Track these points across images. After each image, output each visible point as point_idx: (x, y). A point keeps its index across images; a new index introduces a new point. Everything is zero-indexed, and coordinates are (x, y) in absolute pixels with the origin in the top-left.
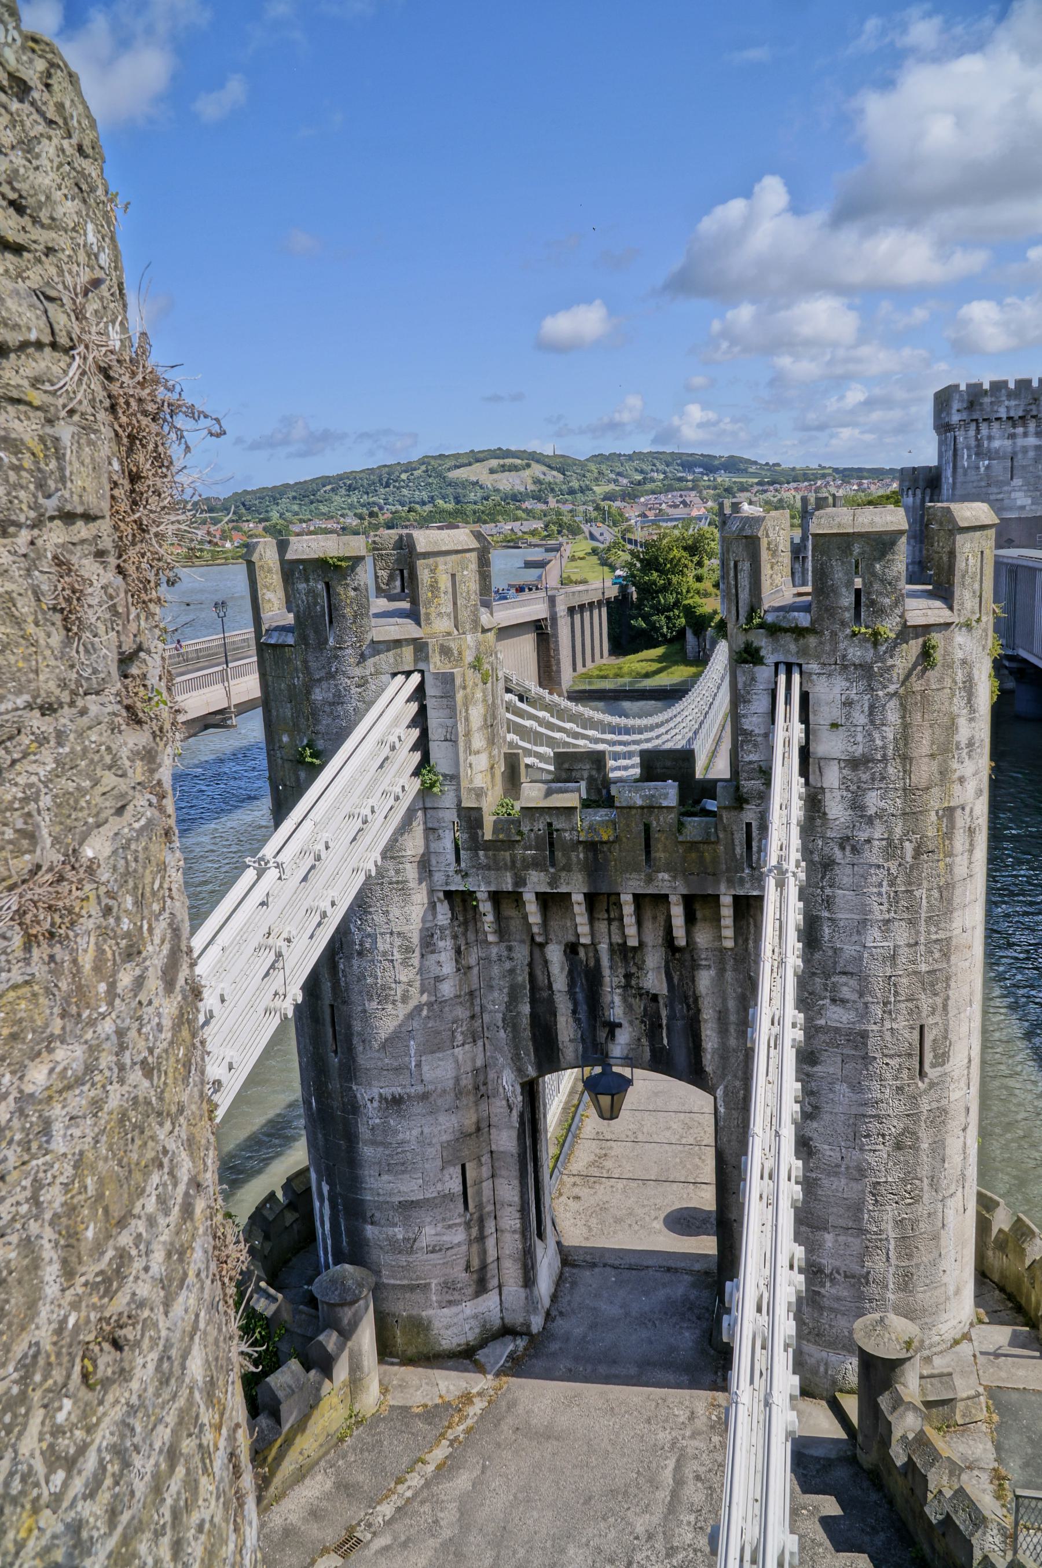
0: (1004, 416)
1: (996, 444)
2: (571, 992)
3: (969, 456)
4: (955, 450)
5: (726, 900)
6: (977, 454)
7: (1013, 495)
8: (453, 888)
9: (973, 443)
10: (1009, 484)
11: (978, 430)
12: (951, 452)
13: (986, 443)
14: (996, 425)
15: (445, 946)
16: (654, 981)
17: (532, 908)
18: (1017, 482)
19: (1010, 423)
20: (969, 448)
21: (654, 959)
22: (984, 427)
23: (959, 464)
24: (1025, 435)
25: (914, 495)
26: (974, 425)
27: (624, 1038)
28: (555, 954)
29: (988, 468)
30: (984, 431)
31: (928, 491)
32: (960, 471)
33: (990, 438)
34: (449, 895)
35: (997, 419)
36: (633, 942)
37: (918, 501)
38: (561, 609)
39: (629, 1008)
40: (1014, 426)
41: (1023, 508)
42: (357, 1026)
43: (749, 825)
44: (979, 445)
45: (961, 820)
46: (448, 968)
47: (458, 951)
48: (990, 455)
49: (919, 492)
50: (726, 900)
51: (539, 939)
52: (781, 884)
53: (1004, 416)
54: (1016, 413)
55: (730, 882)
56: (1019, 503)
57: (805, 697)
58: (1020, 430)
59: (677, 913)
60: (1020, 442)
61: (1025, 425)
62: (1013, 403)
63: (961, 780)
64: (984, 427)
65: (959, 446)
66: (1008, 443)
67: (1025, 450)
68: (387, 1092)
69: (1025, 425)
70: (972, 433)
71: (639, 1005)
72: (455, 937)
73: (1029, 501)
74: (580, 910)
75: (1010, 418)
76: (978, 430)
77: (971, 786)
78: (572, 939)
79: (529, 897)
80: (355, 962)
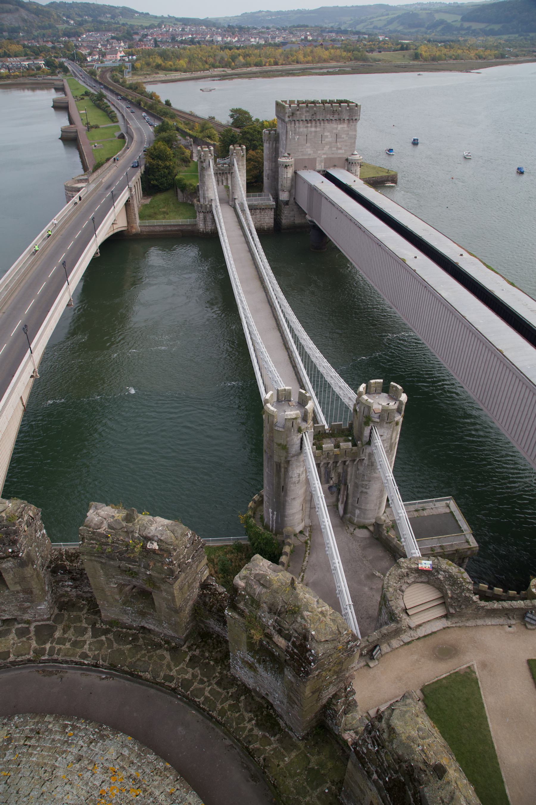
0: (304, 119)
1: (301, 130)
2: (325, 474)
3: (292, 134)
4: (287, 131)
6: (295, 133)
9: (293, 129)
11: (295, 124)
12: (285, 131)
14: (301, 122)
16: (340, 470)
18: (308, 145)
19: (306, 122)
22: (297, 123)
23: (288, 137)
24: (311, 127)
25: (269, 143)
27: (333, 479)
29: (298, 139)
30: (297, 125)
31: (275, 142)
32: (288, 140)
33: (299, 127)
37: (271, 146)
39: (335, 474)
40: (308, 123)
41: (310, 154)
42: (288, 489)
44: (295, 130)
48: (300, 134)
49: (271, 142)
53: (304, 119)
54: (309, 118)
56: (309, 152)
58: (309, 125)
60: (309, 129)
61: (311, 123)
62: (308, 114)
64: (297, 123)
65: (288, 130)
66: (305, 129)
67: (311, 132)
68: (292, 498)
69: (311, 123)
70: (293, 125)
71: (337, 474)
73: (312, 152)
75: (306, 120)
76: (295, 124)
80: (290, 480)
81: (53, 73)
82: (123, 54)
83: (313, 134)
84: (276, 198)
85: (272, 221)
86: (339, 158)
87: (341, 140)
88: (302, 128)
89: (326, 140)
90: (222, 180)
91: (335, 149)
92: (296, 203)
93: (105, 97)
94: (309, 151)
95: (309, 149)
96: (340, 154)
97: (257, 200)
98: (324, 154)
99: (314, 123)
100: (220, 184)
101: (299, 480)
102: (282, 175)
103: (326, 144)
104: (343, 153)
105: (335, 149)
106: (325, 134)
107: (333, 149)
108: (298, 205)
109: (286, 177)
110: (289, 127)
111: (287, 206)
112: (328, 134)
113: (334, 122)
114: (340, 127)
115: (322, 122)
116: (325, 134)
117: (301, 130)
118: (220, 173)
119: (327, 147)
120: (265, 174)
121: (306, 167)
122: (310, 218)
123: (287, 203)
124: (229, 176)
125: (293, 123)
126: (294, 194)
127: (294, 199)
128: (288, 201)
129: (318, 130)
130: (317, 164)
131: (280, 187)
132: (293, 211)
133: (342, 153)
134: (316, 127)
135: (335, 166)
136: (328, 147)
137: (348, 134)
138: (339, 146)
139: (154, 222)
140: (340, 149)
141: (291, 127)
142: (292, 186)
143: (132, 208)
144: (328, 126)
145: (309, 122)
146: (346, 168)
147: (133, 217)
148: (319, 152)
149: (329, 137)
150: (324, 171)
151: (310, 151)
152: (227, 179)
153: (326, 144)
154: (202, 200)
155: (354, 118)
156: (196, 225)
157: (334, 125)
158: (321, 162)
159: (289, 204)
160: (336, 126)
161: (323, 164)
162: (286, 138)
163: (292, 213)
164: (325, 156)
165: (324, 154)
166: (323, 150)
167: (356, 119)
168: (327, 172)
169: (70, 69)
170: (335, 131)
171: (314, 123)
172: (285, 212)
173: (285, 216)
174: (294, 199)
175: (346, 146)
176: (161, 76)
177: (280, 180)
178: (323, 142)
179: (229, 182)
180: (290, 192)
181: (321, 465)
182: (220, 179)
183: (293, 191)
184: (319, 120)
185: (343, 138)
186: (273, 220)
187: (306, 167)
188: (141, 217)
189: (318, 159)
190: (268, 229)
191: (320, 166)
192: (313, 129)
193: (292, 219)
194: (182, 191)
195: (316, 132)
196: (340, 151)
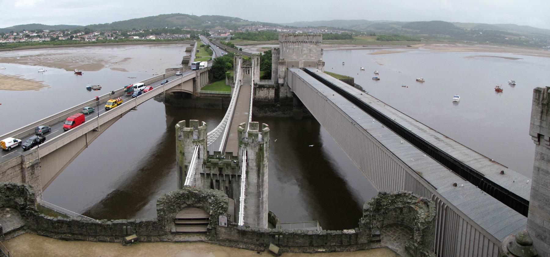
5: (237, 175)
6: (287, 48)
7: (294, 57)
8: (201, 172)
9: (286, 46)
10: (293, 54)
11: (287, 44)
13: (288, 46)
14: (290, 43)
15: (200, 180)
17: (212, 175)
18: (294, 54)
19: (293, 43)
20: (285, 47)
21: (227, 182)
24: (296, 45)
25: (275, 54)
26: (286, 43)
28: (214, 181)
29: (289, 51)
30: (288, 44)
31: (277, 54)
33: (289, 45)
34: (201, 173)
35: (291, 42)
36: (225, 180)
38: (199, 75)
41: (295, 59)
43: (240, 166)
44: (287, 46)
45: (265, 165)
46: (200, 183)
47: (201, 180)
50: (237, 175)
51: (212, 179)
52: (243, 183)
55: (237, 173)
56: (295, 58)
57: (247, 151)
58: (295, 44)
59: (231, 177)
60: (295, 46)
61: (296, 43)
63: (265, 161)
64: (288, 43)
67: (296, 48)
69: (296, 43)
70: (286, 44)
72: (201, 179)
73: (296, 58)
74: (218, 176)
75: (293, 42)
76: (287, 44)
77: (266, 161)
78: (217, 179)
79: (211, 174)
81: (192, 39)
82: (229, 34)
83: (297, 49)
84: (277, 82)
85: (274, 95)
86: (312, 62)
87: (313, 52)
88: (291, 46)
89: (304, 52)
90: (246, 71)
91: (310, 57)
92: (288, 85)
93: (210, 46)
94: (294, 58)
95: (295, 57)
96: (312, 60)
97: (265, 83)
98: (303, 59)
99: (297, 43)
100: (245, 73)
101: (195, 185)
102: (280, 69)
103: (305, 54)
104: (314, 59)
106: (304, 49)
107: (308, 57)
108: (289, 87)
109: (281, 70)
110: (283, 45)
111: (282, 87)
112: (305, 49)
113: (309, 43)
114: (312, 46)
115: (302, 43)
116: (304, 49)
117: (290, 47)
118: (245, 67)
119: (305, 56)
120: (272, 71)
121: (293, 66)
122: (292, 91)
123: (283, 85)
124: (250, 69)
125: (286, 43)
126: (287, 80)
127: (287, 83)
128: (283, 84)
129: (299, 47)
130: (300, 65)
131: (278, 76)
132: (286, 89)
133: (314, 59)
134: (298, 45)
135: (310, 66)
136: (306, 56)
137: (316, 49)
138: (312, 56)
139: (209, 92)
140: (312, 57)
141: (285, 45)
142: (285, 76)
143: (197, 83)
144: (305, 45)
145: (295, 43)
146: (316, 67)
147: (197, 88)
148: (301, 58)
149: (306, 51)
150: (304, 68)
151: (295, 57)
152: (249, 71)
153: (305, 54)
154: (234, 81)
156: (230, 95)
157: (308, 45)
158: (302, 63)
159: (284, 85)
160: (309, 45)
161: (303, 65)
162: (282, 50)
163: (285, 91)
164: (304, 61)
165: (303, 59)
166: (303, 57)
168: (305, 69)
169: (200, 38)
170: (309, 48)
171: (297, 43)
172: (282, 90)
173: (282, 92)
174: (287, 83)
175: (316, 56)
176: (245, 42)
177: (278, 72)
178: (302, 53)
179: (250, 72)
180: (284, 78)
181: (212, 175)
182: (245, 71)
183: (286, 79)
184: (300, 42)
185: (314, 51)
186: (274, 94)
187: (293, 66)
188: (202, 89)
189: (300, 62)
190: (271, 99)
191: (301, 66)
192: (297, 46)
193: (286, 94)
194: (228, 79)
195: (298, 48)
196: (312, 58)
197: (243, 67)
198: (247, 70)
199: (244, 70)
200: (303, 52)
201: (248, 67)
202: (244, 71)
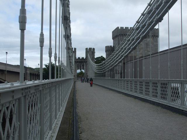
76: (123, 37)
89: (141, 46)
90: (81, 66)
91: (146, 51)
100: (79, 68)
105: (146, 51)
110: (119, 38)
118: (79, 62)
119: (142, 51)
124: (85, 64)
125: (122, 36)
137: (153, 44)
140: (149, 51)
152: (83, 66)
155: (156, 35)
167: (157, 36)
197: (77, 62)
198: (81, 65)
199: (78, 65)
200: (140, 47)
201: (83, 62)
202: (78, 67)
